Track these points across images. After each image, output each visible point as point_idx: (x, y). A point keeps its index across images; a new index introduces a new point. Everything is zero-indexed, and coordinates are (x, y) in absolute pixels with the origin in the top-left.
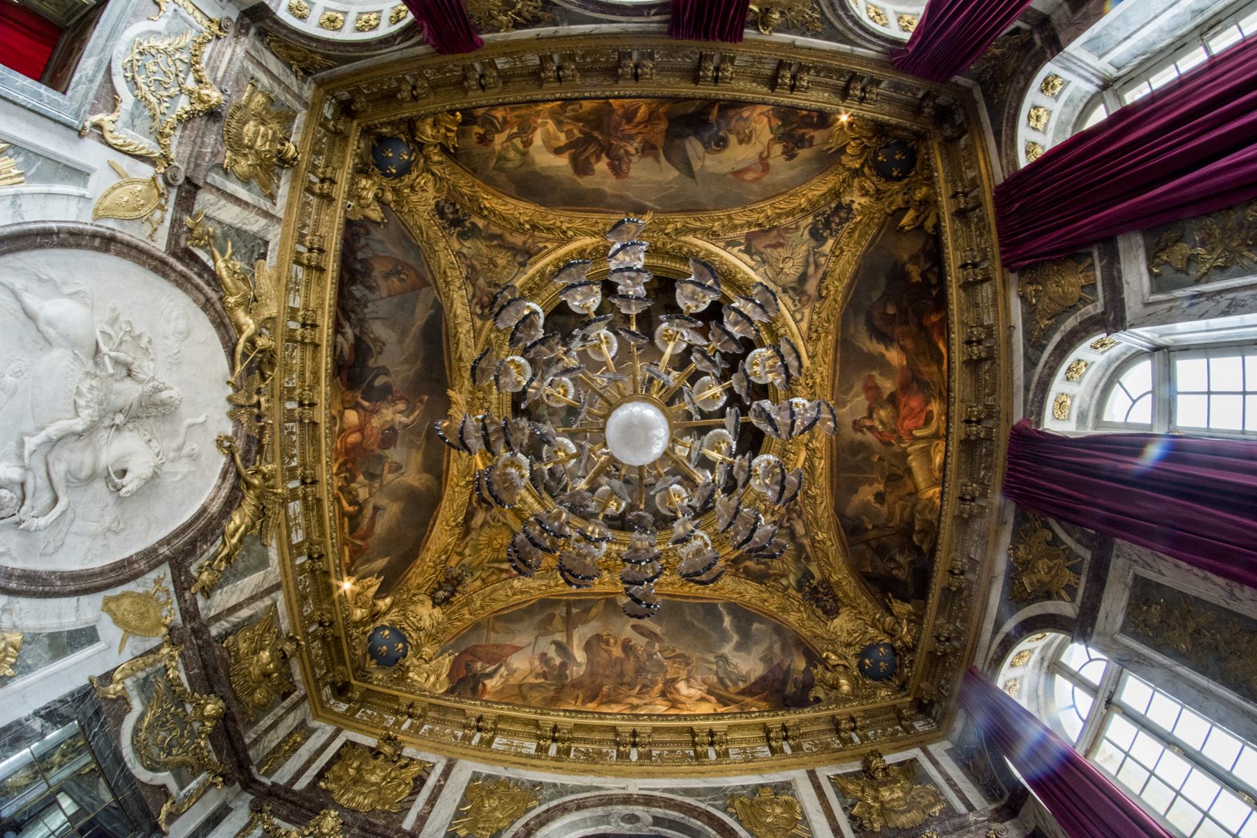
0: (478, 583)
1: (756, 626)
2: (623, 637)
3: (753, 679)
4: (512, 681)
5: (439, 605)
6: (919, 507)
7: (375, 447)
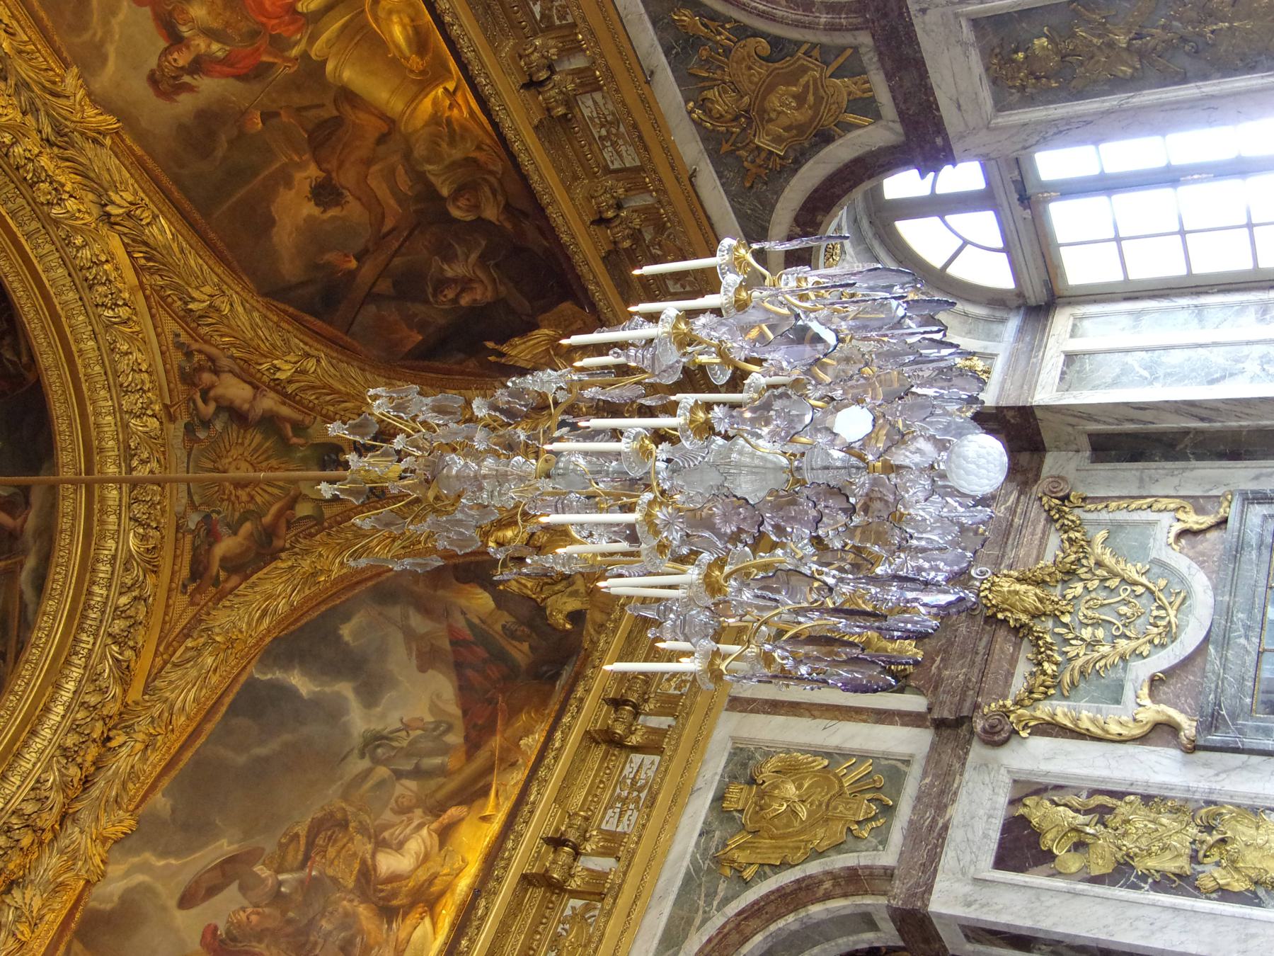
1: (346, 632)
6: (420, 150)
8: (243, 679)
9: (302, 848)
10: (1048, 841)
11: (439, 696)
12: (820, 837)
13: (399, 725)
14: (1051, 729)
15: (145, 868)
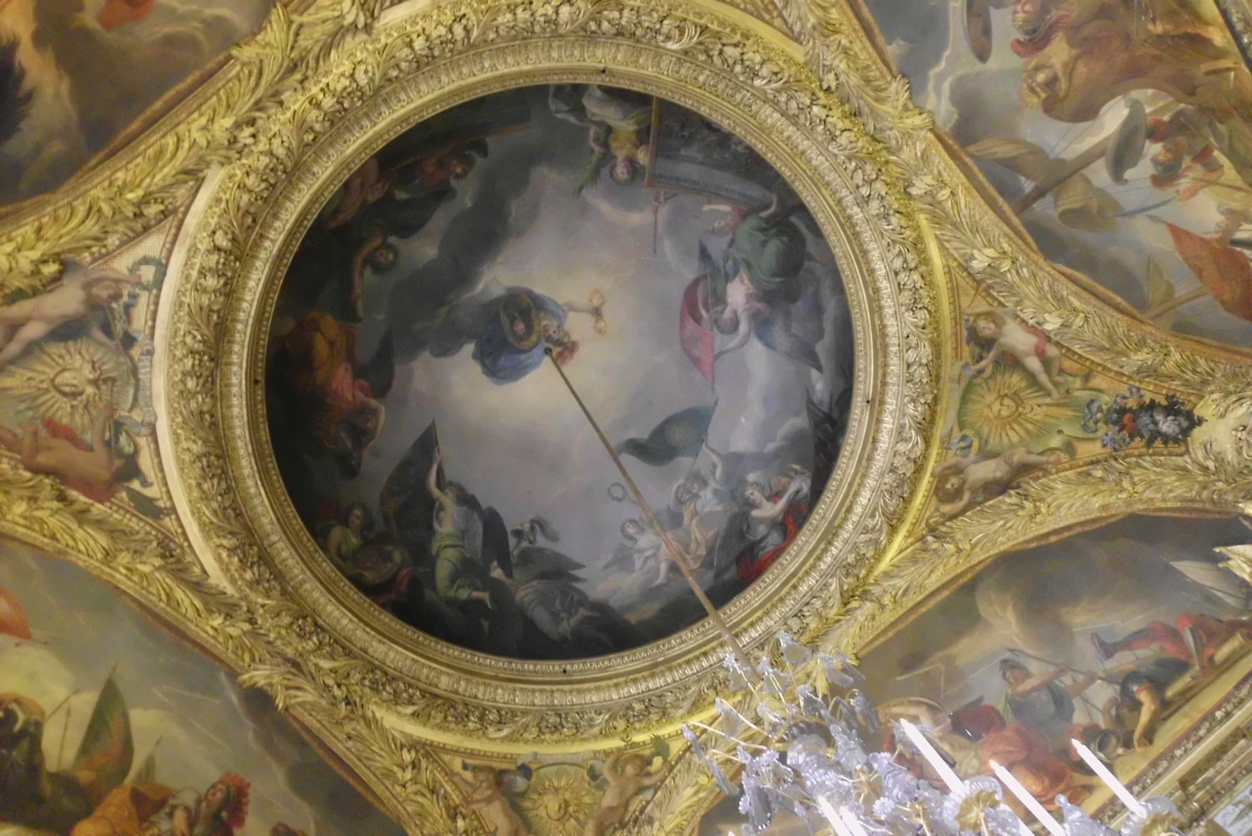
0: (1098, 381)
2: (1015, 62)
5: (1189, 415)
7: (1008, 733)
15: (941, 78)
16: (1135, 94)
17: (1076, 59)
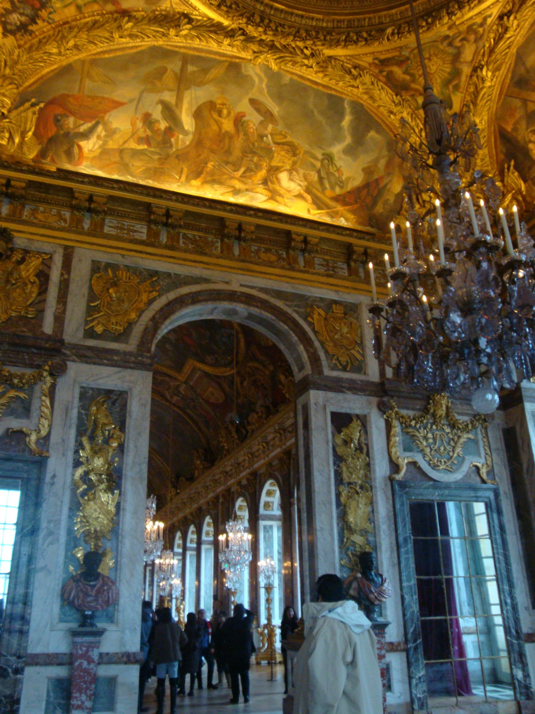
1: (372, 134)
3: (349, 187)
4: (112, 145)
8: (344, 96)
9: (282, 141)
10: (345, 431)
11: (354, 179)
12: (330, 346)
13: (338, 166)
14: (389, 426)
15: (261, 80)
16: (190, 137)
17: (220, 129)
